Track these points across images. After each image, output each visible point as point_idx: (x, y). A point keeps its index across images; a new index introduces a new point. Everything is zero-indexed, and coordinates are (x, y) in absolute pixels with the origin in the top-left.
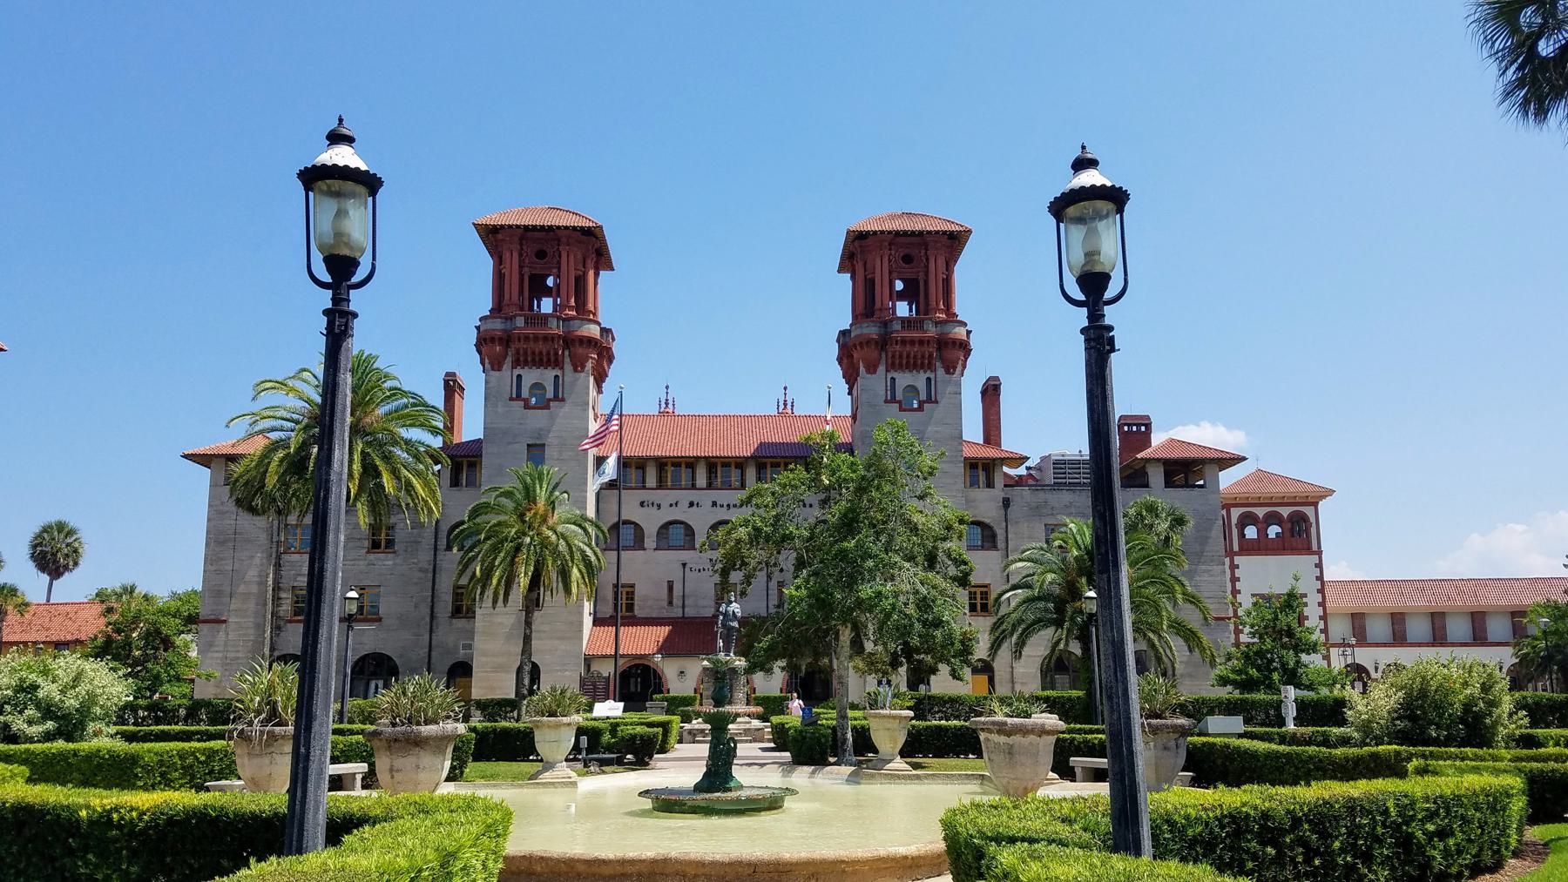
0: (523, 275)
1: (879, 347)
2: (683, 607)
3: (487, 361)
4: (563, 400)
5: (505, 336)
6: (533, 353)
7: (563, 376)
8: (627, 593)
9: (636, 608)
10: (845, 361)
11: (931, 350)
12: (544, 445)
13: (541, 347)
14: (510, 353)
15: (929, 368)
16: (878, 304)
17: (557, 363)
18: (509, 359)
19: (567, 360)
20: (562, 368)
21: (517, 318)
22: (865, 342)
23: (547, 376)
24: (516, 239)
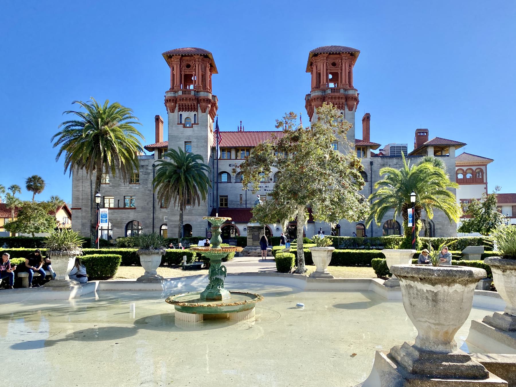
0: (182, 75)
1: (322, 100)
2: (246, 204)
3: (168, 109)
4: (198, 124)
5: (175, 99)
7: (198, 114)
8: (225, 199)
9: (228, 204)
10: (308, 107)
11: (343, 101)
12: (191, 142)
13: (189, 103)
14: (177, 106)
15: (342, 109)
16: (322, 83)
17: (195, 109)
18: (177, 108)
19: (199, 108)
20: (197, 111)
21: (179, 91)
22: (316, 99)
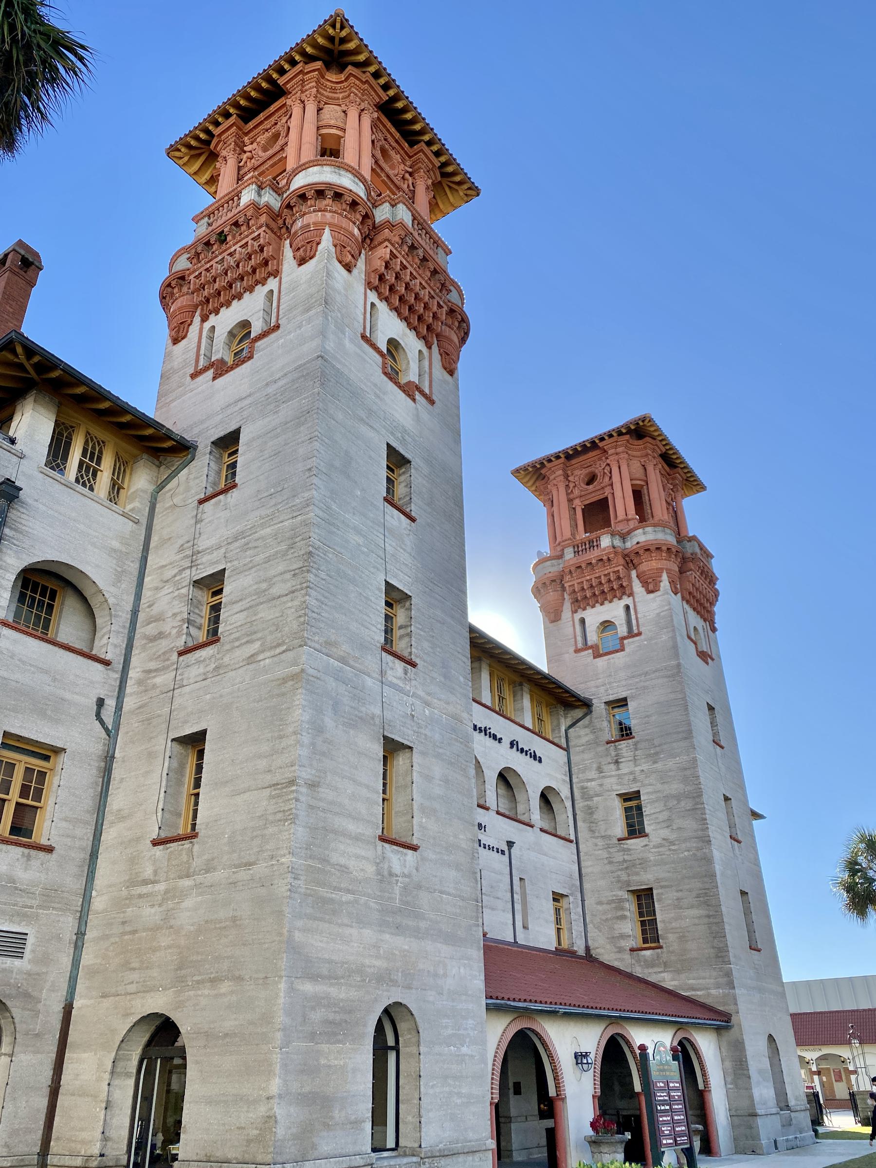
0: (574, 509)
6: (592, 586)
14: (566, 596)
17: (624, 590)
20: (631, 595)
21: (566, 551)
23: (614, 611)
24: (560, 472)
